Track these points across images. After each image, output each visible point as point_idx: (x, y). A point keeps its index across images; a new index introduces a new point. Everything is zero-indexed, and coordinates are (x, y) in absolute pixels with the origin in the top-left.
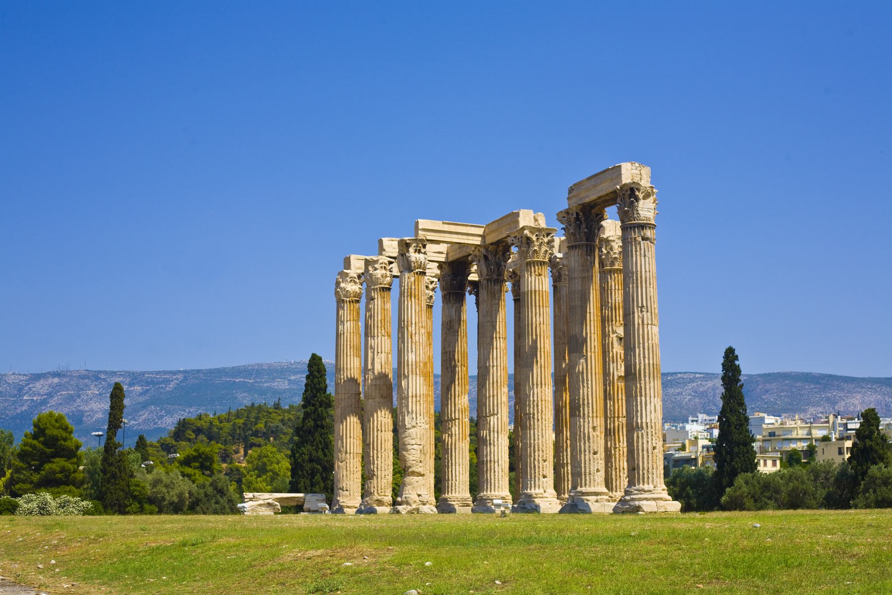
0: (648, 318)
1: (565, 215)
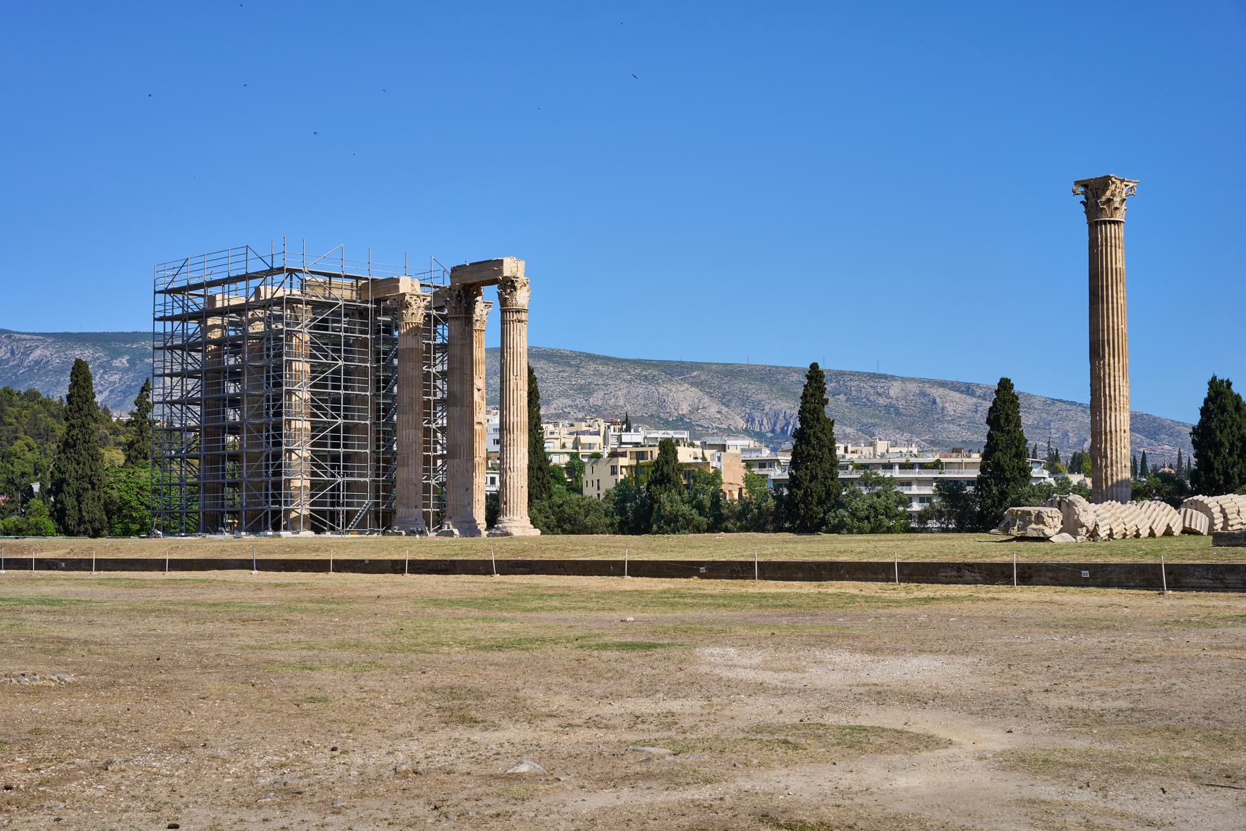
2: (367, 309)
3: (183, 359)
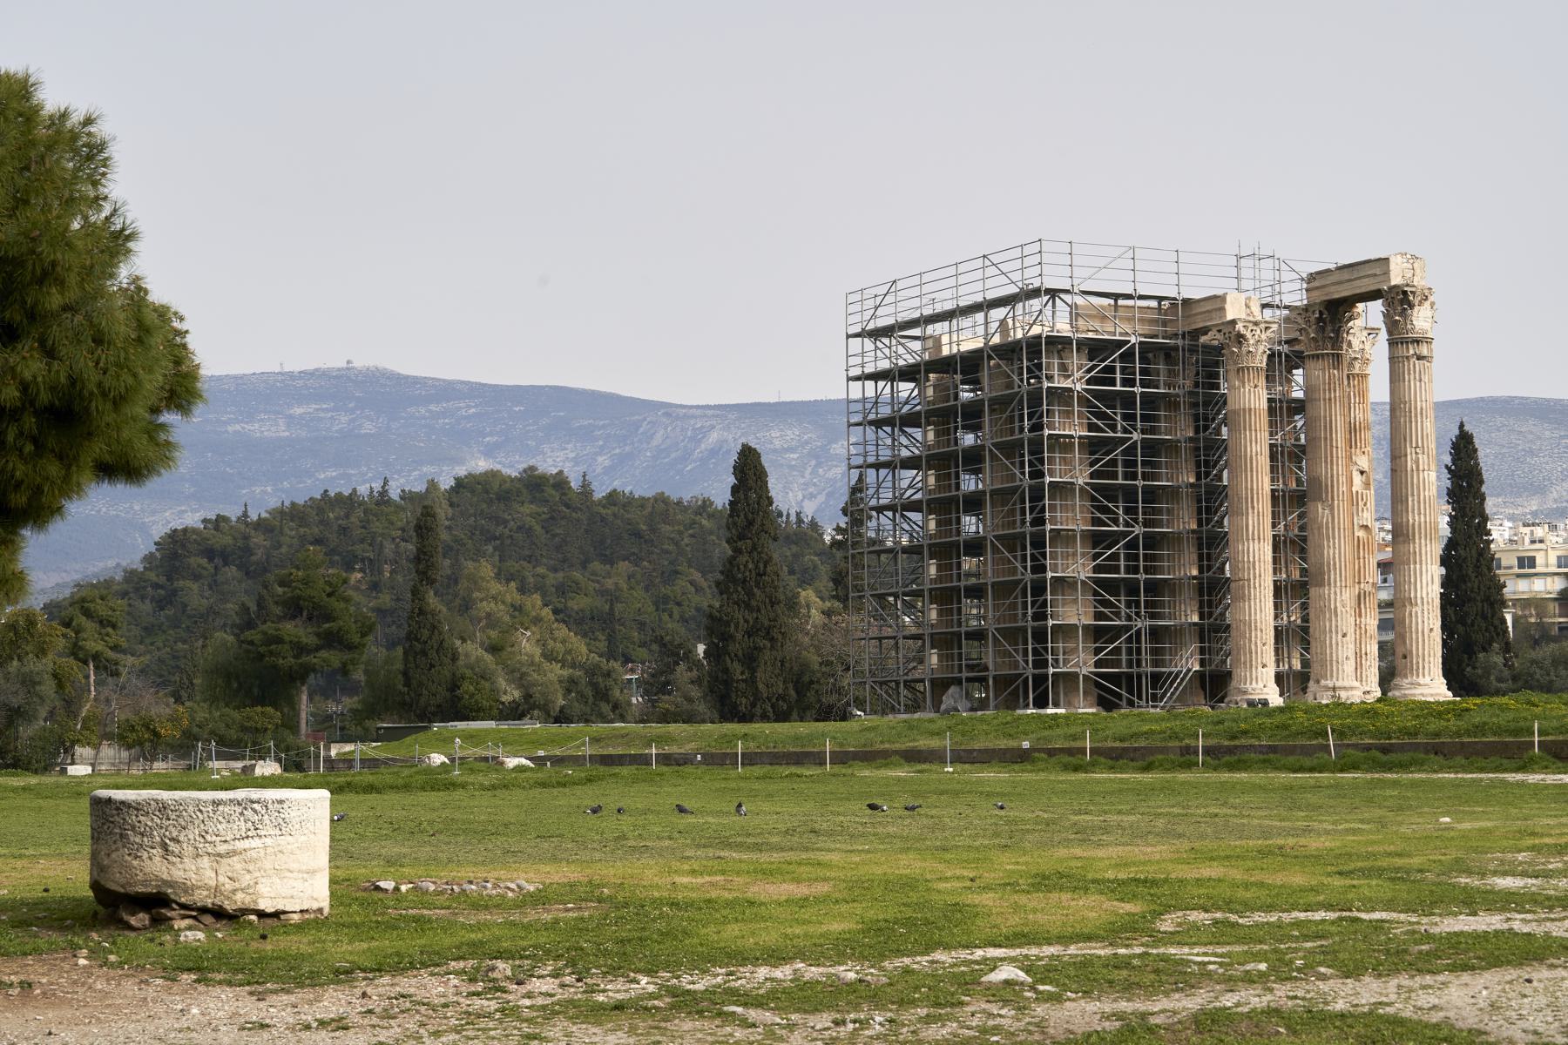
2: (1176, 348)
3: (894, 440)
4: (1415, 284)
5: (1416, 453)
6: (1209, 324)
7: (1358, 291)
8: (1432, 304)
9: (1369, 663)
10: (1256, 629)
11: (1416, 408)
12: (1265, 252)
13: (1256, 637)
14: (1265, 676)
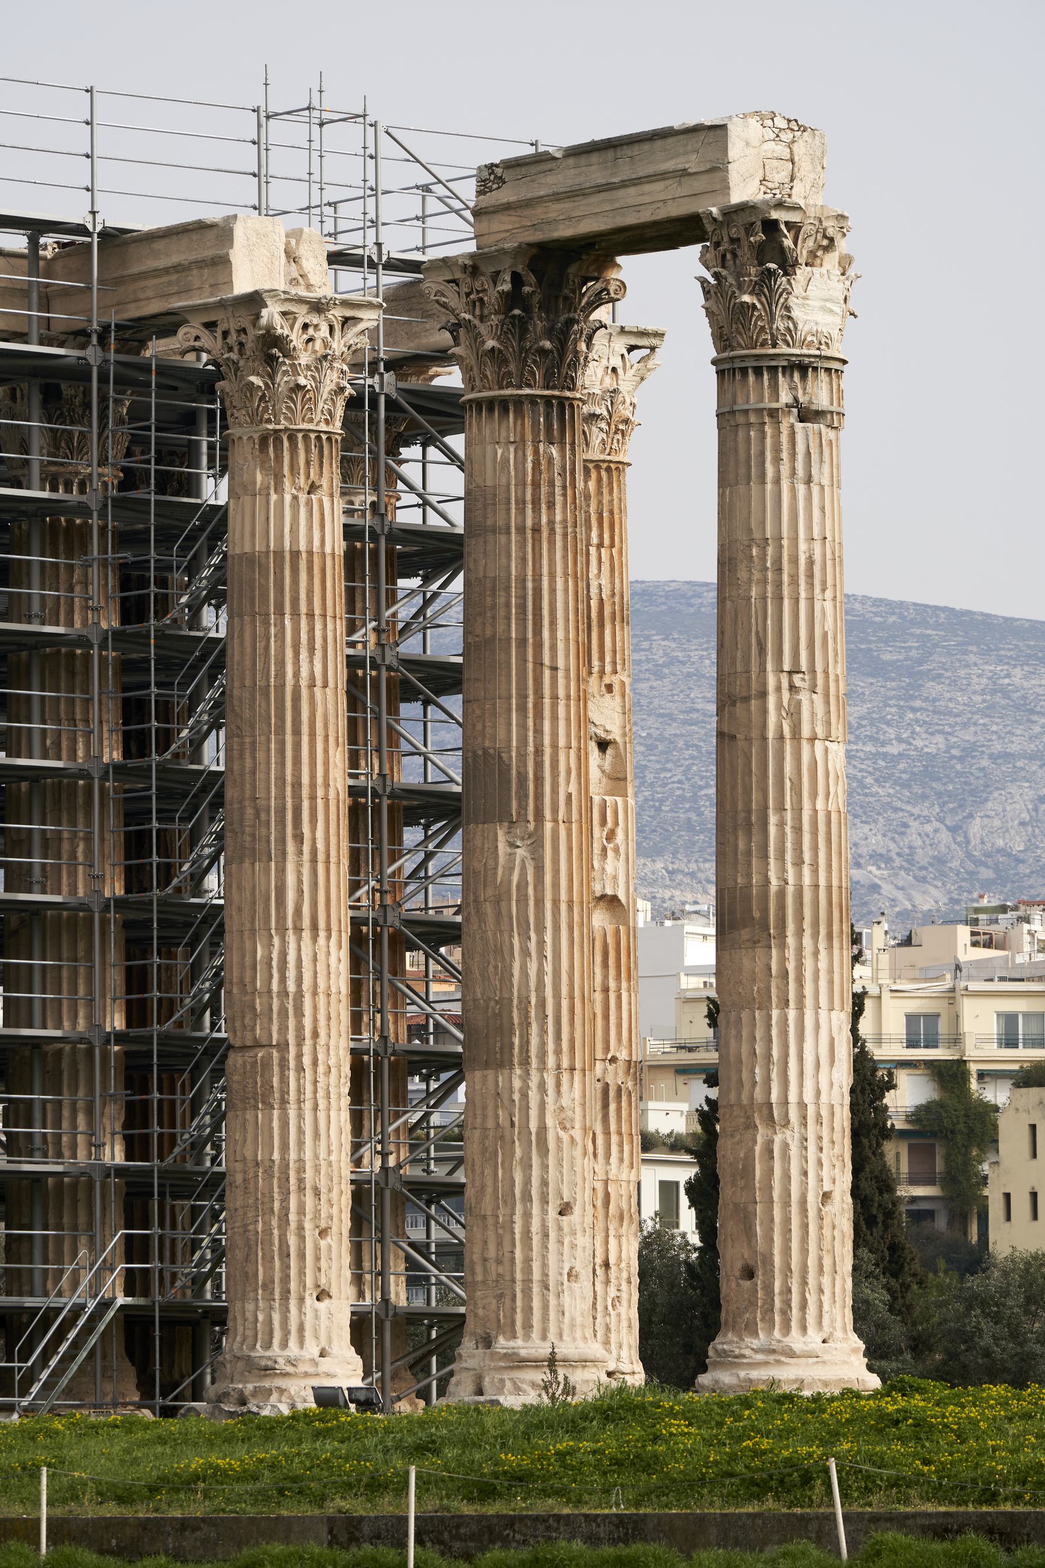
0: (813, 714)
1: (458, 275)
2: (79, 373)
4: (797, 199)
5: (792, 688)
6: (178, 304)
7: (631, 219)
8: (845, 263)
9: (612, 1292)
10: (301, 1189)
11: (794, 560)
12: (335, 102)
13: (301, 1211)
14: (324, 1322)
